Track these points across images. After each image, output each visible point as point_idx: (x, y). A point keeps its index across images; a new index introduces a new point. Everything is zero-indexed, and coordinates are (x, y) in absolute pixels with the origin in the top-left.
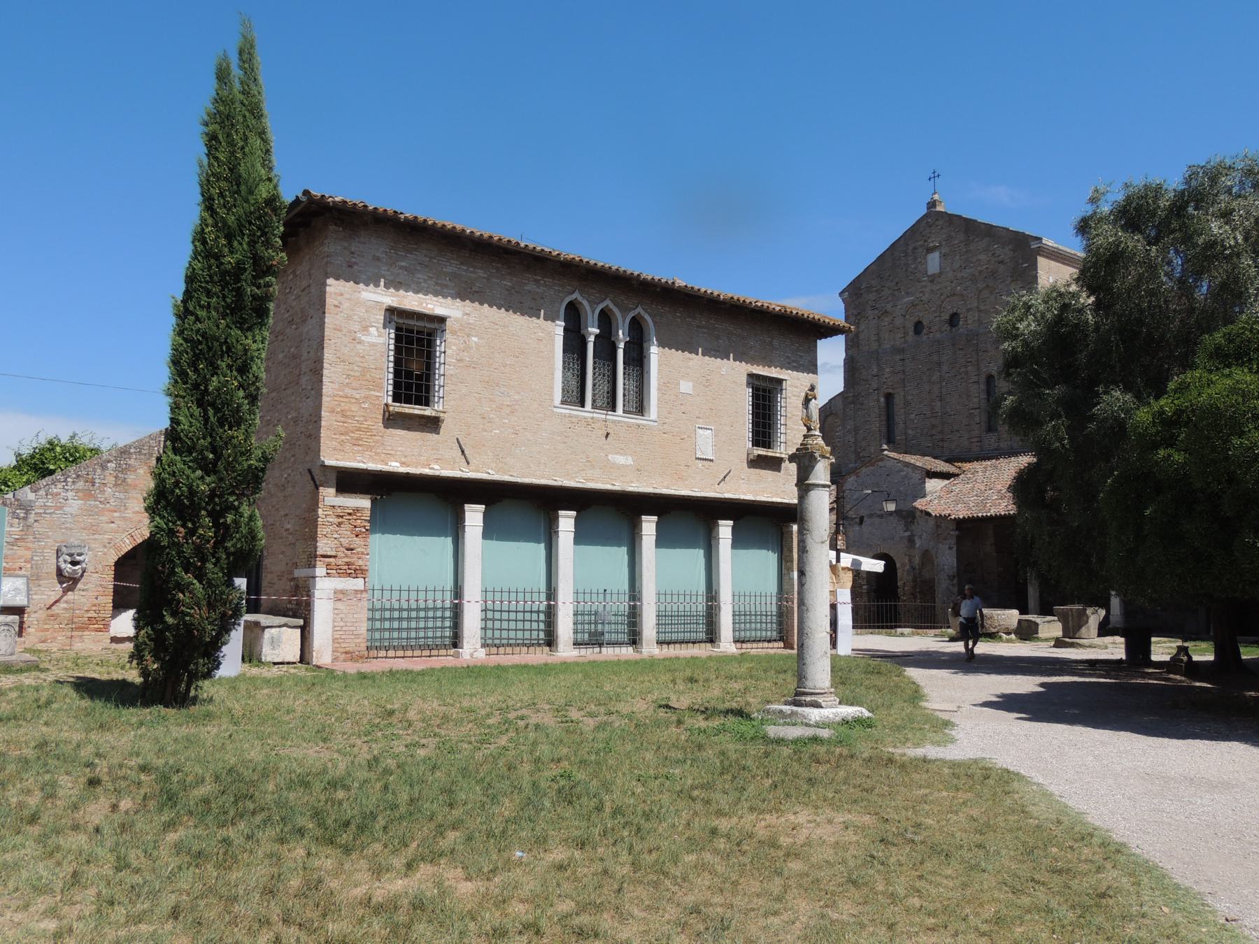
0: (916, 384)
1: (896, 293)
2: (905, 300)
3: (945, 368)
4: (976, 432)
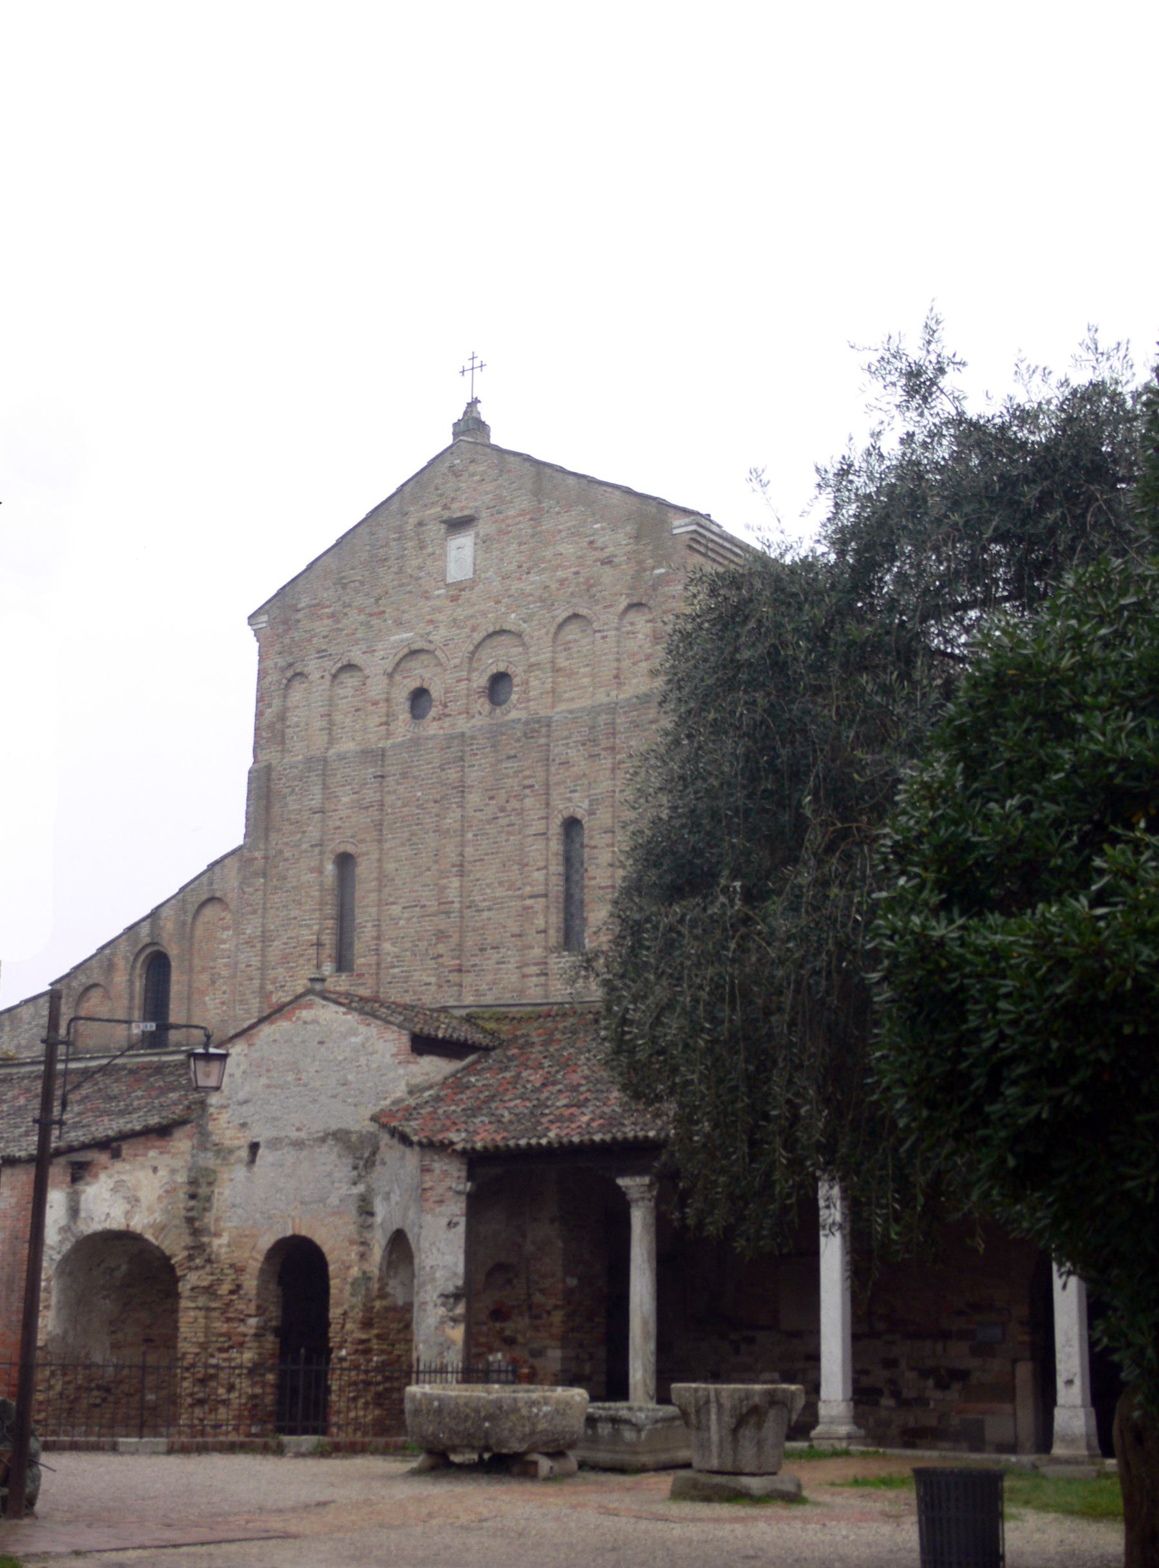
0: (406, 835)
1: (375, 621)
2: (393, 638)
3: (474, 798)
4: (537, 952)
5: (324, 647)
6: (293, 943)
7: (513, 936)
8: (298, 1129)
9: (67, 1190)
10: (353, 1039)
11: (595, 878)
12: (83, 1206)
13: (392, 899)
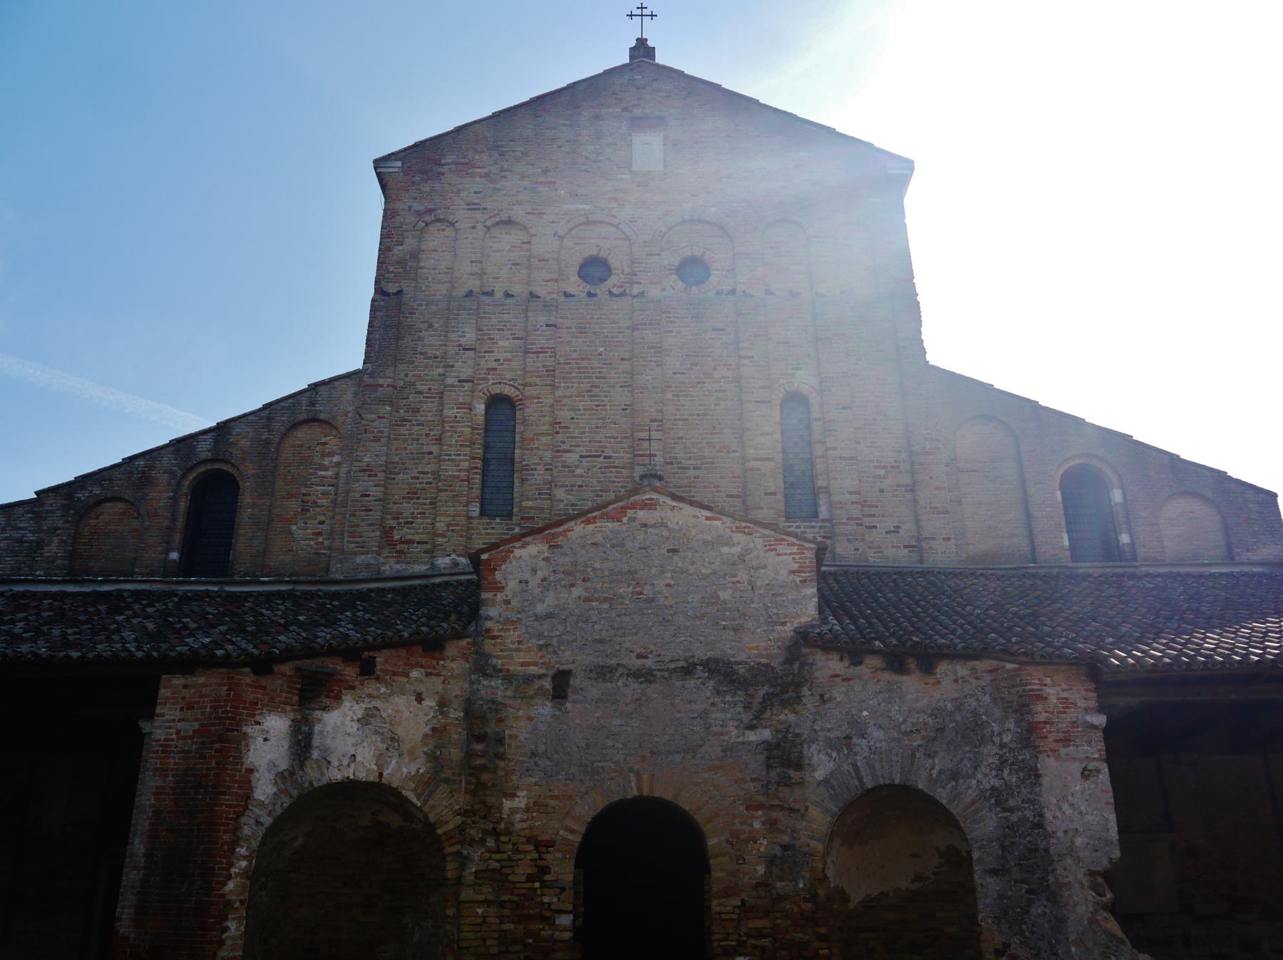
5: (478, 201)
6: (429, 478)
7: (727, 496)
8: (639, 656)
9: (292, 715)
10: (725, 550)
11: (835, 449)
12: (316, 742)
13: (564, 447)
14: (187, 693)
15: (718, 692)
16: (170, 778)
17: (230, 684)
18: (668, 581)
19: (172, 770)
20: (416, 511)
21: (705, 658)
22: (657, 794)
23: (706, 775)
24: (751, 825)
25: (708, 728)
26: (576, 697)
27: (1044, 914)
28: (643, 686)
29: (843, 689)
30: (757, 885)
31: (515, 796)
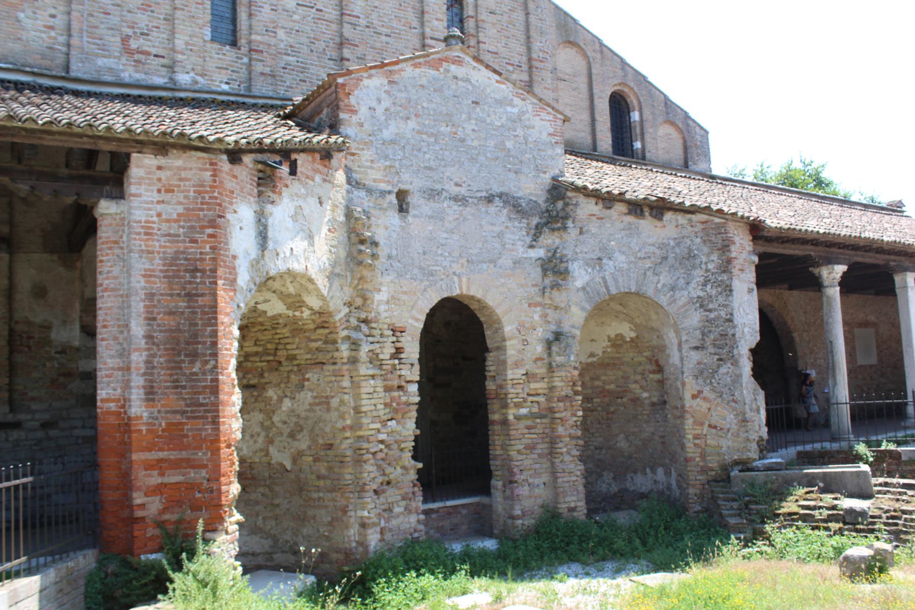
8: (457, 185)
10: (509, 109)
11: (485, 43)
14: (163, 175)
15: (510, 219)
16: (157, 261)
17: (215, 170)
18: (473, 127)
19: (159, 253)
20: (151, 24)
21: (498, 191)
22: (472, 293)
23: (503, 280)
24: (532, 317)
25: (503, 246)
26: (415, 212)
27: (728, 373)
28: (461, 208)
29: (597, 225)
30: (537, 359)
31: (380, 290)
